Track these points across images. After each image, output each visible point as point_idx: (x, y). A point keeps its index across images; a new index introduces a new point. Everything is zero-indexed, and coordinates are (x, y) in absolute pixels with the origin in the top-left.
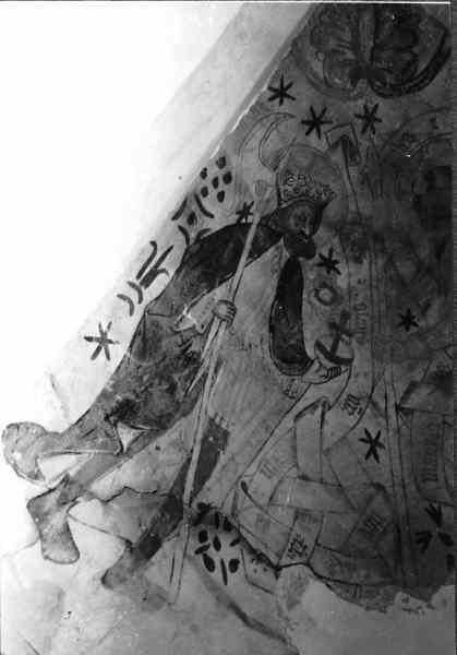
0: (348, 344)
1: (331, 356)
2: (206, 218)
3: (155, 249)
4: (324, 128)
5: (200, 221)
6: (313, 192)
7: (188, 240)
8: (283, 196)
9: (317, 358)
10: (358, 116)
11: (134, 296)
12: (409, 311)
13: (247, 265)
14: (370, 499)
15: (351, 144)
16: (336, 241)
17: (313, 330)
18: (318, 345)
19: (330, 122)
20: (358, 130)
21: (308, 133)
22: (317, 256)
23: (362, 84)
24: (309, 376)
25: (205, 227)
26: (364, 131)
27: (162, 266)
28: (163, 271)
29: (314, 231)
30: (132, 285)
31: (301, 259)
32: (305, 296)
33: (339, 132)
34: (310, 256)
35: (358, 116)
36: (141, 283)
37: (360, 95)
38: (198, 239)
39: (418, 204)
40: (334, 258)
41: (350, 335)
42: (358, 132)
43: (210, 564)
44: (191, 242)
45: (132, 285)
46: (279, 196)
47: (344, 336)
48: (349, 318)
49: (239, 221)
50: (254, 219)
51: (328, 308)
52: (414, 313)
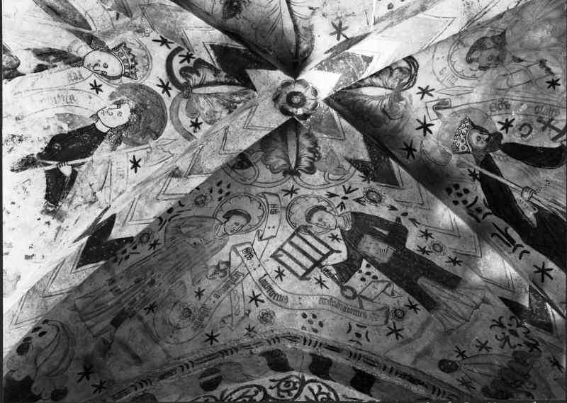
0: (557, 122)
2: (478, 201)
3: (497, 235)
5: (480, 206)
6: (464, 131)
7: (489, 214)
8: (465, 150)
9: (561, 142)
10: (422, 98)
11: (520, 250)
12: (548, 82)
13: (502, 177)
15: (438, 104)
18: (554, 139)
19: (425, 117)
21: (431, 133)
22: (501, 132)
23: (404, 94)
25: (482, 202)
26: (431, 95)
27: (503, 230)
28: (506, 229)
29: (486, 132)
30: (514, 251)
31: (503, 142)
32: (524, 143)
33: (431, 111)
34: (501, 136)
35: (422, 98)
36: (513, 245)
37: (410, 96)
38: (489, 207)
40: (504, 122)
41: (552, 120)
44: (490, 211)
45: (514, 251)
46: (465, 152)
47: (552, 123)
48: (541, 118)
49: (477, 179)
50: (478, 169)
51: (533, 130)
52: (550, 80)
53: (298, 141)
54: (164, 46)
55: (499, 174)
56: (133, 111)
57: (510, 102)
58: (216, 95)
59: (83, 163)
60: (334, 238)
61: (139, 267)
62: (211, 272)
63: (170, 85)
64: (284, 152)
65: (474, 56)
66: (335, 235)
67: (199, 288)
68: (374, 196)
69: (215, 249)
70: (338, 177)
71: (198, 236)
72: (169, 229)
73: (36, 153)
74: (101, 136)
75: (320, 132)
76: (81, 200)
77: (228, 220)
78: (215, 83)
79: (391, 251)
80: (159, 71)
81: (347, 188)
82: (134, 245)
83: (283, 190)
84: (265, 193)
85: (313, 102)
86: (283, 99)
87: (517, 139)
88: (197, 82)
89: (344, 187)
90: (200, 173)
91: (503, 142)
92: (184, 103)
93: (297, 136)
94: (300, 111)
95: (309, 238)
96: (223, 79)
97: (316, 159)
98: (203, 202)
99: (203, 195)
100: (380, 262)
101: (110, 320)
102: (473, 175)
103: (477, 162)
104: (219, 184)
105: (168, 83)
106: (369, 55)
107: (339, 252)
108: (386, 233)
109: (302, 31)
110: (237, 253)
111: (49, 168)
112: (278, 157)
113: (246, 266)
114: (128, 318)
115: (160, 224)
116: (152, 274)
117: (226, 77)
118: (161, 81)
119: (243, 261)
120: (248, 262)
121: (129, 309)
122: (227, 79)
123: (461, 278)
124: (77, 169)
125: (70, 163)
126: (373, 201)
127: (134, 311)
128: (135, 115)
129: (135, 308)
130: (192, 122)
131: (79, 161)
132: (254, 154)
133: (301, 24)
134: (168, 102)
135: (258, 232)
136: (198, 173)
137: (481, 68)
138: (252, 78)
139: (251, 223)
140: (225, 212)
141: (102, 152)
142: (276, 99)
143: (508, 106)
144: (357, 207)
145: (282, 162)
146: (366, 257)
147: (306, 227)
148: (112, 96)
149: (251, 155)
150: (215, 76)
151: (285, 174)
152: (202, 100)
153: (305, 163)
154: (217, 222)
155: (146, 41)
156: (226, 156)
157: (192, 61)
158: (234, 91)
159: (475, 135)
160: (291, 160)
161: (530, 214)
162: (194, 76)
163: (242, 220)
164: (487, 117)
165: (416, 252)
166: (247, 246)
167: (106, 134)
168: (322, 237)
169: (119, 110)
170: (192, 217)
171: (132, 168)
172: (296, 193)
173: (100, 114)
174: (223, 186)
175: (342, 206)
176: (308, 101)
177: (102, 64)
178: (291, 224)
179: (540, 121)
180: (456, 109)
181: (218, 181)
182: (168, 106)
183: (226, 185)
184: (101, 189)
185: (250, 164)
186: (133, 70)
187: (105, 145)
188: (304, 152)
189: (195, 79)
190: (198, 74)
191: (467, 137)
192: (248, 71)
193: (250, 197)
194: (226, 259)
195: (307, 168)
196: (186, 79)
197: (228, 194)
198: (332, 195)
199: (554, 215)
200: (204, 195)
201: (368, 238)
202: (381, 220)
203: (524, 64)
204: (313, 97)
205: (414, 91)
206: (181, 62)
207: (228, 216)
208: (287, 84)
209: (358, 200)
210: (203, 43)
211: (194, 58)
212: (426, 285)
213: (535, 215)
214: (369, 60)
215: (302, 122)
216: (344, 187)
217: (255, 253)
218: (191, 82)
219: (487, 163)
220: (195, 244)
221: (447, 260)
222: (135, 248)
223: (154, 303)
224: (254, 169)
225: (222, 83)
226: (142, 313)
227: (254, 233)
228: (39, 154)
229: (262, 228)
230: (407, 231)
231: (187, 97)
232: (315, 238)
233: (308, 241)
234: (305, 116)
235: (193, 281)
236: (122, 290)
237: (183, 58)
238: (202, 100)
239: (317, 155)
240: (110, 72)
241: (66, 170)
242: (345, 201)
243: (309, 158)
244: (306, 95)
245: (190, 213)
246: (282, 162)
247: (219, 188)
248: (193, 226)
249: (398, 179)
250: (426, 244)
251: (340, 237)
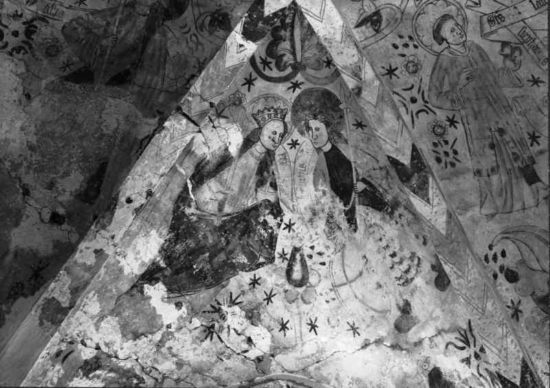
54: (254, 82)
56: (315, 117)
58: (303, 41)
59: (356, 170)
61: (475, 142)
62: (509, 63)
63: (294, 81)
67: (528, 81)
69: (481, 56)
71: (459, 74)
72: (438, 104)
73: (344, 208)
74: (334, 148)
76: (384, 182)
77: (446, 40)
80: (280, 89)
82: (442, 142)
88: (291, 57)
92: (309, 71)
96: (288, 34)
98: (416, 65)
99: (407, 65)
101: (525, 185)
104: (395, 47)
105: (292, 83)
110: (492, 33)
111: (357, 200)
113: (512, 24)
114: (535, 166)
115: (427, 113)
116: (491, 129)
117: (286, 31)
118: (289, 88)
119: (505, 26)
120: (508, 22)
121: (522, 162)
122: (288, 30)
124: (360, 178)
125: (355, 182)
127: (528, 157)
128: (319, 116)
129: (525, 156)
130: (326, 66)
131: (354, 173)
132: (365, 8)
134: (307, 86)
135: (468, 7)
139: (454, 14)
140: (434, 42)
141: (348, 152)
148: (302, 133)
149: (365, 12)
150: (284, 41)
152: (307, 55)
154: (445, 52)
155: (249, 97)
157: (269, 59)
158: (299, 23)
162: (285, 59)
163: (448, 25)
166: (485, 19)
167: (332, 145)
169: (313, 129)
170: (431, 78)
171: (363, 129)
173: (317, 147)
174: (398, 42)
177: (272, 136)
181: (391, 47)
182: (312, 86)
183: (399, 39)
184: (378, 161)
185: (377, 13)
186: (279, 111)
187: (342, 147)
189: (288, 58)
190: (284, 55)
193: (419, 15)
194: (498, 47)
196: (288, 66)
197: (411, 38)
200: (405, 63)
206: (271, 69)
207: (439, 38)
211: (266, 58)
217: (496, 12)
218: (290, 62)
220: (468, 79)
222: (446, 142)
223: (529, 134)
224: (383, 8)
225: (292, 35)
226: (536, 148)
227: (468, 12)
228: (345, 205)
231: (304, 68)
235: (515, 86)
236: (495, 164)
237: (266, 68)
238: (307, 55)
240: (280, 130)
241: (360, 186)
245: (426, 80)
247: (401, 47)
248: (444, 78)
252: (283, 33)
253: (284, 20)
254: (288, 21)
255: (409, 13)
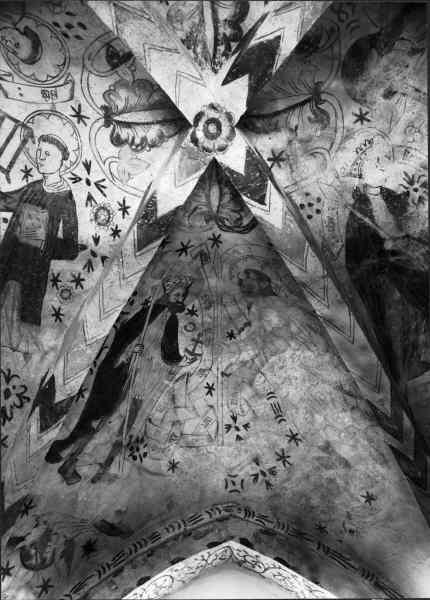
1: (192, 353)
4: (189, 250)
10: (210, 239)
14: (207, 412)
16: (196, 302)
17: (184, 343)
18: (186, 350)
20: (210, 246)
23: (212, 223)
24: (182, 363)
31: (178, 314)
32: (179, 329)
33: (198, 250)
35: (210, 239)
37: (211, 229)
39: (240, 283)
42: (210, 248)
43: (135, 458)
53: (153, 123)
55: (150, 322)
57: (212, 309)
58: (202, 21)
60: (27, 173)
64: (135, 107)
65: (252, 275)
66: (31, 173)
68: (103, 217)
70: (115, 173)
75: (181, 160)
77: (22, 33)
78: (216, 21)
79: (40, 245)
81: (102, 184)
83: (80, 106)
84: (74, 83)
85: (211, 147)
86: (212, 114)
87: (181, 324)
89: (104, 180)
90: (118, 20)
91: (178, 314)
93: (158, 122)
94: (200, 135)
95: (16, 142)
96: (221, 30)
97: (134, 147)
100: (17, 233)
102: (147, 301)
103: (158, 301)
106: (267, 201)
107: (9, 180)
108: (60, 234)
109: (274, 120)
112: (127, 100)
117: (224, 35)
122: (222, 36)
123: (39, 324)
126: (96, 217)
133: (281, 119)
136: (117, 19)
137: (241, 280)
138: (239, 80)
139: (22, 66)
140: (34, 29)
142: (212, 107)
143: (208, 308)
144: (80, 193)
145: (121, 105)
146: (17, 215)
147: (32, 136)
149: (129, 68)
150: (226, 20)
151: (104, 108)
153: (124, 133)
156: (142, 51)
158: (208, 43)
159: (180, 291)
160: (125, 115)
161: (122, 359)
163: (25, 50)
164: (197, 295)
165: (50, 272)
168: (22, 157)
172: (79, 122)
174: (81, 32)
175: (76, 179)
176: (212, 142)
178: (32, 117)
179: (199, 335)
180: (201, 270)
181: (88, 26)
185: (114, 67)
188: (140, 132)
191: (178, 285)
192: (246, 77)
193: (64, 64)
195: (118, 136)
197: (66, 36)
198: (88, 166)
199: (126, 376)
201: (44, 215)
202: (75, 227)
203: (247, 311)
204: (216, 147)
205: (217, 231)
208: (229, 117)
209: (90, 198)
210: (283, 28)
212: (12, 291)
213: (123, 363)
214: (262, 201)
215: (189, 137)
216: (104, 180)
219: (158, 308)
221: (56, 307)
225: (216, 29)
229: (16, 79)
230: (72, 258)
232: (19, 150)
233: (12, 141)
234: (195, 140)
239: (139, 148)
242: (84, 182)
243: (133, 139)
244: (219, 139)
246: (121, 105)
249: (144, 250)
250: (66, 281)
251: (30, 180)
252: (228, 31)
253: (226, 48)
254: (222, 48)
255: (76, 65)
